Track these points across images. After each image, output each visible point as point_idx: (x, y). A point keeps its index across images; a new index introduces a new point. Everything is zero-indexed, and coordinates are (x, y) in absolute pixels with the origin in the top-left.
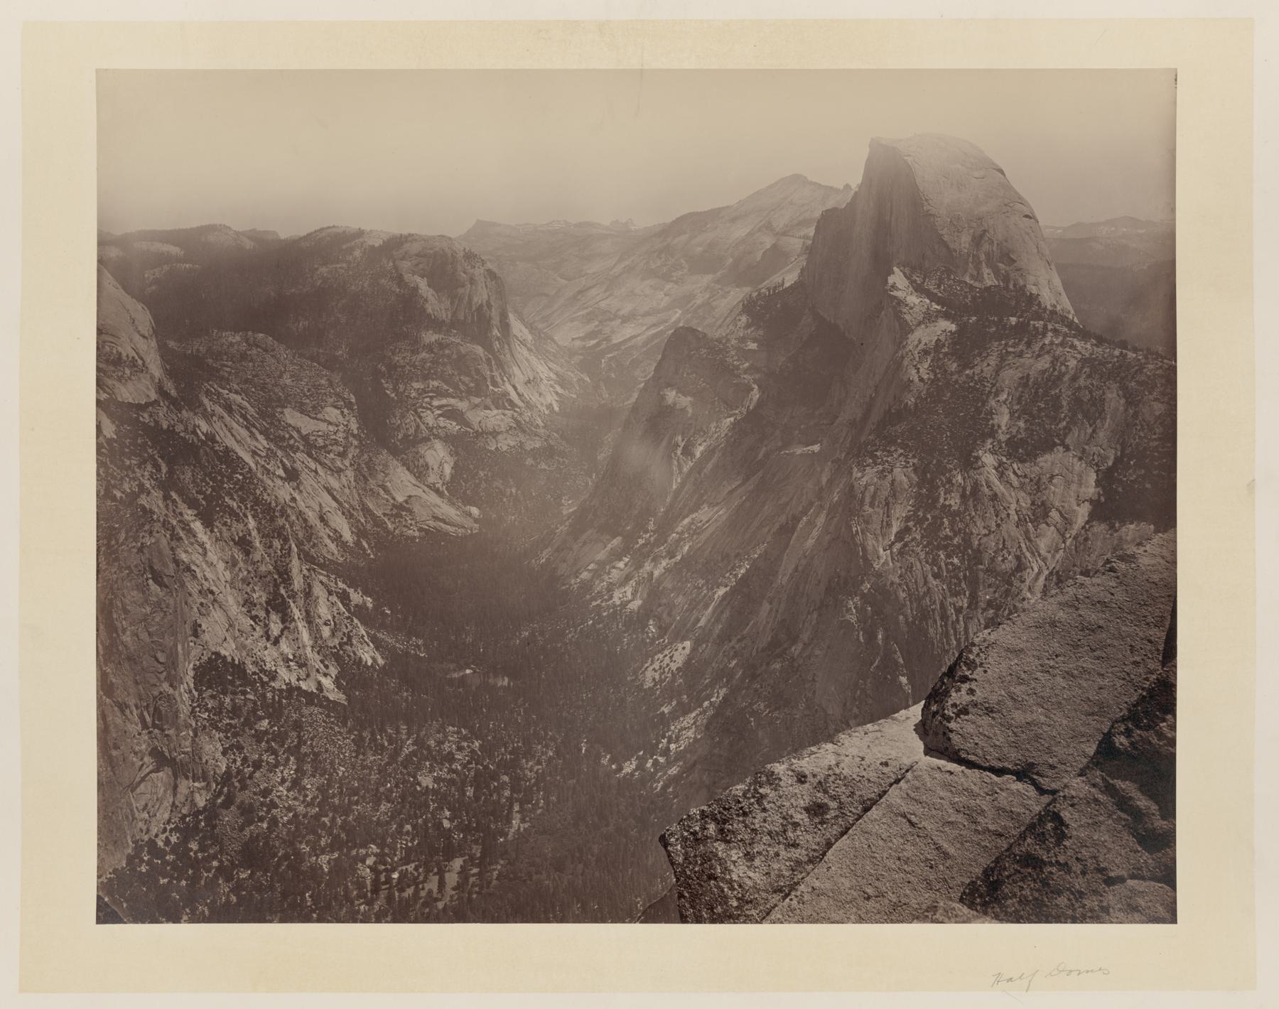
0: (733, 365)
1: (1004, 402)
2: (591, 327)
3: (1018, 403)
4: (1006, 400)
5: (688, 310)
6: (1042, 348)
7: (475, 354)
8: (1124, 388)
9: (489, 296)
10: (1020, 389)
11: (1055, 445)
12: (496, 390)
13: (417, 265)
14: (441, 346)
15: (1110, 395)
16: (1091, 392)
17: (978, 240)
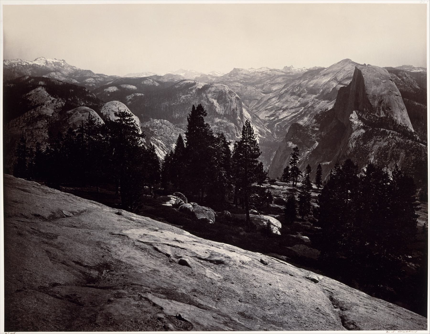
0: (310, 135)
1: (373, 154)
2: (272, 113)
3: (377, 155)
4: (374, 153)
5: (306, 108)
6: (386, 139)
7: (232, 126)
8: (406, 151)
9: (236, 106)
10: (378, 151)
11: (385, 166)
12: (238, 137)
13: (213, 95)
14: (221, 123)
15: (402, 153)
16: (396, 152)
17: (380, 103)
